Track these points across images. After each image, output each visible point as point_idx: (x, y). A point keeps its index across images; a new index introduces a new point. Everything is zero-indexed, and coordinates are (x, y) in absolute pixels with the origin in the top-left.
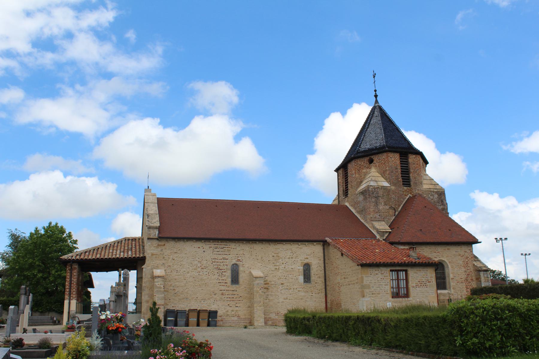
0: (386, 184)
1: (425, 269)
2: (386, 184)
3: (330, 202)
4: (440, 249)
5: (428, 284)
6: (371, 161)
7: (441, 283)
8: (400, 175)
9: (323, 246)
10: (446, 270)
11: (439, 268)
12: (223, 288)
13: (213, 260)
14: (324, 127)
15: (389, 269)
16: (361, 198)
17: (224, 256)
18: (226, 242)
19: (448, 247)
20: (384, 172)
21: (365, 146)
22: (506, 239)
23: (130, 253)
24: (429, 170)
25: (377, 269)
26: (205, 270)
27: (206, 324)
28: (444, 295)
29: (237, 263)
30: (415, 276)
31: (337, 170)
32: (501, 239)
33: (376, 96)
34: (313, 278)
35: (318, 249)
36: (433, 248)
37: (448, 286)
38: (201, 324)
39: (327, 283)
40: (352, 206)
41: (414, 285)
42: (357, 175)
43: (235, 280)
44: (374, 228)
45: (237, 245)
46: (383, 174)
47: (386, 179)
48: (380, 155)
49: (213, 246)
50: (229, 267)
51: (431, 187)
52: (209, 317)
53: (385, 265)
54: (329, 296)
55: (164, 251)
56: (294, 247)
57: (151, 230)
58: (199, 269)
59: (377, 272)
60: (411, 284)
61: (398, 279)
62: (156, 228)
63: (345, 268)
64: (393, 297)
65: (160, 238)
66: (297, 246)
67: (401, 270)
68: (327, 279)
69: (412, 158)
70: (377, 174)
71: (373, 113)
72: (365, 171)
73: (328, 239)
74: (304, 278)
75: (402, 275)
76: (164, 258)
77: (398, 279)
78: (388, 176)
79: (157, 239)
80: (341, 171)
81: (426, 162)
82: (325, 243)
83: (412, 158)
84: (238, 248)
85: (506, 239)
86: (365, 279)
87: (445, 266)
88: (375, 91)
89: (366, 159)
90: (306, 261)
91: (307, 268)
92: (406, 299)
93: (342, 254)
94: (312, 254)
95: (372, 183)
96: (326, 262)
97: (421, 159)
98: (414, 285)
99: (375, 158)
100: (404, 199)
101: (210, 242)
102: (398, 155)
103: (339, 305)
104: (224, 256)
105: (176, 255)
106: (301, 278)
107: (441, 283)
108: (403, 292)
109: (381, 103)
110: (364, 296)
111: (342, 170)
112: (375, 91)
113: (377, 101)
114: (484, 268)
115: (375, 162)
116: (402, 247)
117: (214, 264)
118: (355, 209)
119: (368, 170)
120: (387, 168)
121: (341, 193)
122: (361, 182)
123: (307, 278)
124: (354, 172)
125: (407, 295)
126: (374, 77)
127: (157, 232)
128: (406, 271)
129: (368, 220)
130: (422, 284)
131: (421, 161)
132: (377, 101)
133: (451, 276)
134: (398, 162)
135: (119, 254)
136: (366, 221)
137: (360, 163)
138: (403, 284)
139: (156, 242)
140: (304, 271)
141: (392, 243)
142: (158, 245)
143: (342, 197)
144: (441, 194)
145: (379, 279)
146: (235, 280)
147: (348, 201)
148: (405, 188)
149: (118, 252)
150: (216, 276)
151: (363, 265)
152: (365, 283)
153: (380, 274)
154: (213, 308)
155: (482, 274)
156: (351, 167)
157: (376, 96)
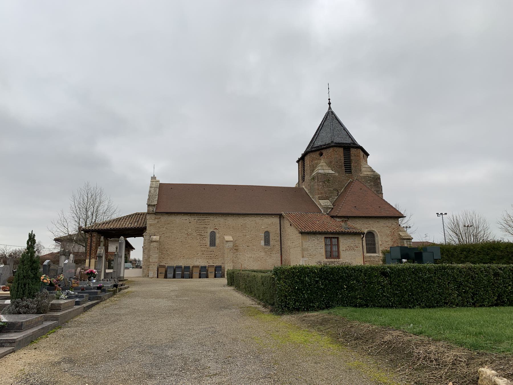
0: (331, 172)
1: (354, 237)
2: (331, 172)
3: (294, 186)
4: (371, 222)
5: (355, 248)
6: (321, 154)
7: (371, 248)
8: (343, 165)
10: (376, 239)
11: (371, 235)
12: (203, 249)
15: (324, 236)
17: (205, 226)
19: (378, 220)
21: (318, 143)
22: (446, 214)
23: (136, 224)
24: (371, 161)
25: (313, 236)
26: (190, 236)
27: (213, 276)
28: (374, 257)
29: (215, 231)
30: (344, 243)
31: (298, 162)
32: (441, 214)
33: (330, 104)
34: (272, 243)
35: (276, 220)
36: (365, 221)
37: (377, 251)
38: (209, 276)
39: (282, 246)
41: (344, 249)
43: (213, 243)
44: (320, 205)
45: (215, 218)
46: (330, 164)
48: (328, 150)
49: (196, 218)
50: (209, 234)
51: (369, 173)
52: (215, 271)
53: (320, 233)
54: (283, 255)
56: (258, 219)
59: (314, 239)
60: (341, 248)
61: (331, 245)
62: (154, 205)
63: (292, 235)
64: (326, 258)
65: (156, 213)
66: (260, 218)
67: (334, 238)
68: (282, 243)
69: (353, 151)
71: (327, 117)
72: (316, 162)
73: (283, 213)
74: (265, 242)
75: (334, 241)
77: (331, 245)
80: (300, 162)
81: (367, 155)
82: (280, 216)
83: (353, 151)
84: (216, 220)
85: (446, 214)
86: (304, 243)
87: (376, 235)
88: (329, 99)
89: (318, 153)
90: (266, 230)
91: (267, 235)
92: (338, 260)
93: (291, 225)
94: (271, 224)
95: (320, 171)
96: (282, 230)
97: (361, 151)
98: (344, 249)
99: (324, 152)
100: (345, 184)
102: (342, 149)
103: (289, 262)
104: (205, 226)
105: (169, 225)
106: (263, 243)
107: (371, 248)
108: (335, 254)
110: (303, 257)
112: (329, 99)
113: (330, 108)
114: (408, 237)
115: (324, 155)
116: (338, 220)
119: (319, 161)
121: (300, 178)
123: (267, 242)
125: (338, 257)
127: (155, 209)
128: (338, 238)
130: (350, 249)
131: (362, 153)
132: (330, 108)
133: (380, 243)
134: (342, 155)
135: (127, 225)
138: (335, 249)
139: (154, 216)
140: (265, 237)
141: (332, 217)
142: (155, 218)
143: (301, 181)
144: (376, 179)
145: (316, 244)
146: (213, 243)
148: (347, 174)
149: (128, 223)
151: (302, 233)
152: (304, 247)
153: (316, 240)
155: (405, 241)
156: (307, 158)
157: (330, 104)
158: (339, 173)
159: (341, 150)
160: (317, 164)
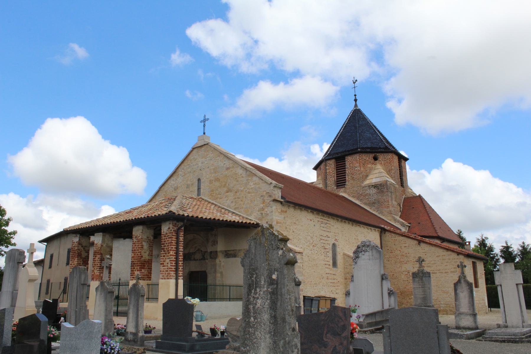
6: (375, 159)
9: (381, 233)
13: (321, 237)
14: (64, 120)
16: (373, 191)
18: (329, 218)
20: (389, 171)
29: (336, 242)
33: (356, 100)
40: (353, 197)
42: (362, 169)
44: (395, 220)
46: (389, 172)
47: (392, 178)
48: (386, 155)
55: (286, 218)
57: (275, 189)
58: (311, 247)
70: (382, 171)
72: (369, 166)
76: (286, 228)
78: (393, 175)
79: (281, 203)
82: (383, 231)
88: (355, 95)
89: (372, 155)
99: (381, 157)
101: (318, 214)
104: (327, 233)
109: (360, 107)
111: (333, 161)
112: (355, 95)
113: (356, 105)
117: (322, 241)
118: (361, 200)
119: (373, 166)
120: (393, 168)
122: (367, 176)
124: (358, 165)
126: (354, 83)
129: (386, 213)
132: (356, 105)
136: (381, 213)
137: (365, 158)
139: (279, 206)
142: (282, 211)
147: (345, 192)
150: (323, 257)
154: (332, 296)
157: (356, 100)
158: (397, 184)
159: (396, 158)
160: (371, 169)
